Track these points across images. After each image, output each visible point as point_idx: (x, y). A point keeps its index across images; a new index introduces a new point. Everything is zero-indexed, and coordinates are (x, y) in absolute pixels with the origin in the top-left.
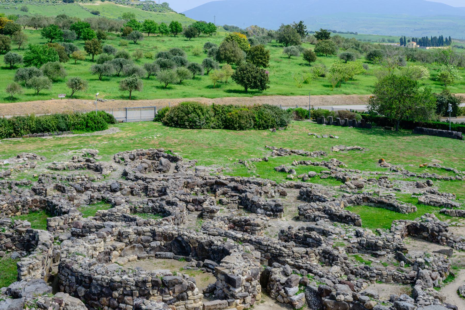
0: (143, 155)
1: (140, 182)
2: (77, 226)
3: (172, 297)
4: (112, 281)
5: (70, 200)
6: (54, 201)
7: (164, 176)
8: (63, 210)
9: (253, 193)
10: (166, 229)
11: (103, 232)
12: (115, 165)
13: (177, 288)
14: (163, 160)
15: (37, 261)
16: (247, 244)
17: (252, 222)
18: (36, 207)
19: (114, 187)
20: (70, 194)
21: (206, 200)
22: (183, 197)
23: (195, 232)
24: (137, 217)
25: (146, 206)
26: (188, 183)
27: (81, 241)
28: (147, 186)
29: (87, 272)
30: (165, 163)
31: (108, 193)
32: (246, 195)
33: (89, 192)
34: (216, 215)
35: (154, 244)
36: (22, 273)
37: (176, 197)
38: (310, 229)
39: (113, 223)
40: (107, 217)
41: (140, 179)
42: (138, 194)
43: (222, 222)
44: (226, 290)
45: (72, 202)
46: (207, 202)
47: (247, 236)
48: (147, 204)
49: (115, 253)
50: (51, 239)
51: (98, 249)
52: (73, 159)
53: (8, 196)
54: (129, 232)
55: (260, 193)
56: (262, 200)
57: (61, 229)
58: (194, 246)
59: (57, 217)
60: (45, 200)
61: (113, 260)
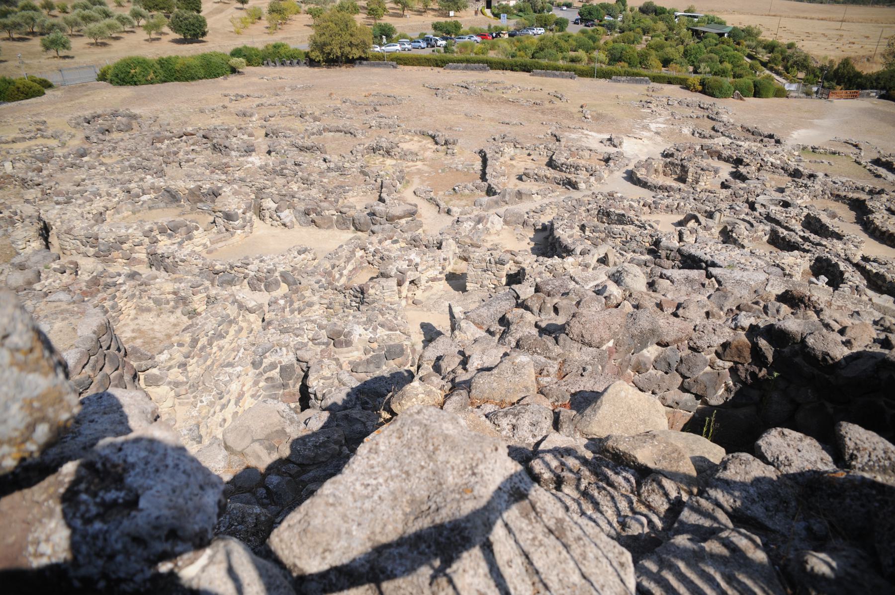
13: (183, 230)
27: (70, 208)
46: (181, 153)
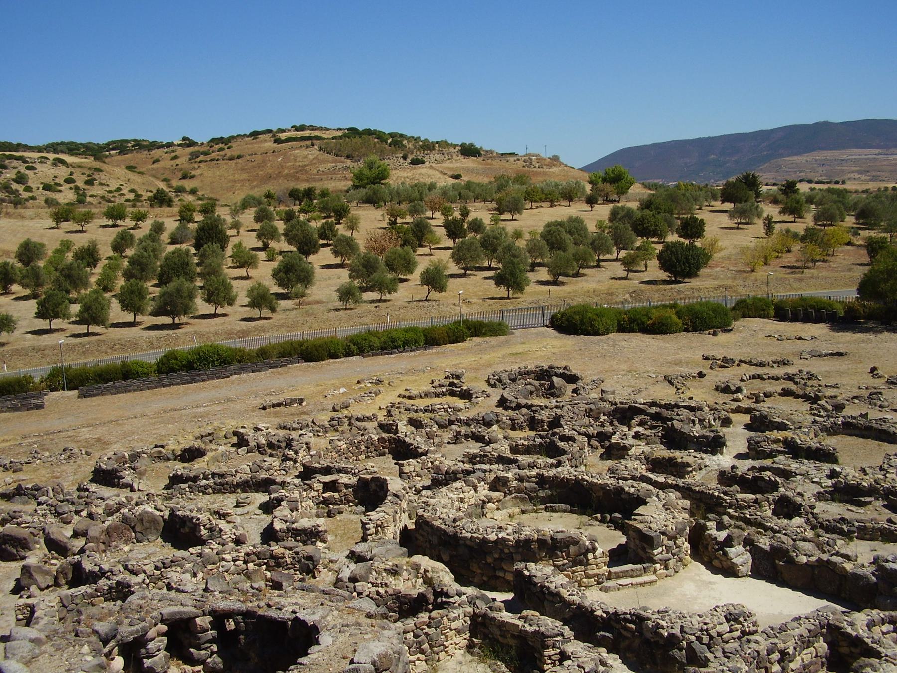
0: (528, 373)
1: (524, 410)
2: (437, 469)
3: (565, 561)
4: (485, 541)
5: (429, 438)
6: (407, 439)
7: (557, 402)
8: (420, 450)
9: (682, 421)
10: (558, 473)
11: (473, 478)
12: (489, 390)
14: (555, 379)
15: (386, 516)
16: (671, 489)
17: (679, 460)
18: (384, 448)
19: (488, 419)
20: (428, 430)
21: (615, 433)
22: (583, 430)
23: (598, 476)
24: (520, 457)
25: (532, 442)
26: (591, 410)
28: (534, 416)
29: (452, 529)
30: (558, 384)
31: (480, 428)
32: (672, 424)
33: (453, 427)
34: (630, 453)
35: (542, 493)
36: (368, 532)
37: (573, 429)
38: (763, 469)
39: (486, 467)
40: (478, 459)
41: (524, 407)
42: (521, 428)
43: (638, 462)
44: (641, 553)
45: (432, 441)
47: (671, 480)
48: (534, 441)
49: (490, 505)
50: (404, 489)
51: (466, 500)
52: (432, 382)
53: (347, 435)
54: (508, 478)
55: (693, 421)
56: (697, 431)
57: (418, 475)
58: (597, 494)
59: (411, 460)
60: (394, 439)
61: (489, 515)
